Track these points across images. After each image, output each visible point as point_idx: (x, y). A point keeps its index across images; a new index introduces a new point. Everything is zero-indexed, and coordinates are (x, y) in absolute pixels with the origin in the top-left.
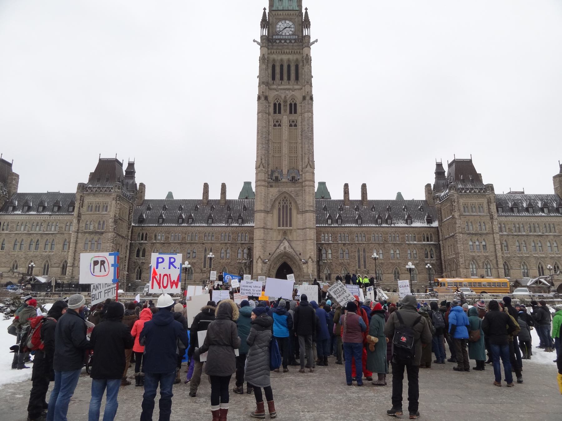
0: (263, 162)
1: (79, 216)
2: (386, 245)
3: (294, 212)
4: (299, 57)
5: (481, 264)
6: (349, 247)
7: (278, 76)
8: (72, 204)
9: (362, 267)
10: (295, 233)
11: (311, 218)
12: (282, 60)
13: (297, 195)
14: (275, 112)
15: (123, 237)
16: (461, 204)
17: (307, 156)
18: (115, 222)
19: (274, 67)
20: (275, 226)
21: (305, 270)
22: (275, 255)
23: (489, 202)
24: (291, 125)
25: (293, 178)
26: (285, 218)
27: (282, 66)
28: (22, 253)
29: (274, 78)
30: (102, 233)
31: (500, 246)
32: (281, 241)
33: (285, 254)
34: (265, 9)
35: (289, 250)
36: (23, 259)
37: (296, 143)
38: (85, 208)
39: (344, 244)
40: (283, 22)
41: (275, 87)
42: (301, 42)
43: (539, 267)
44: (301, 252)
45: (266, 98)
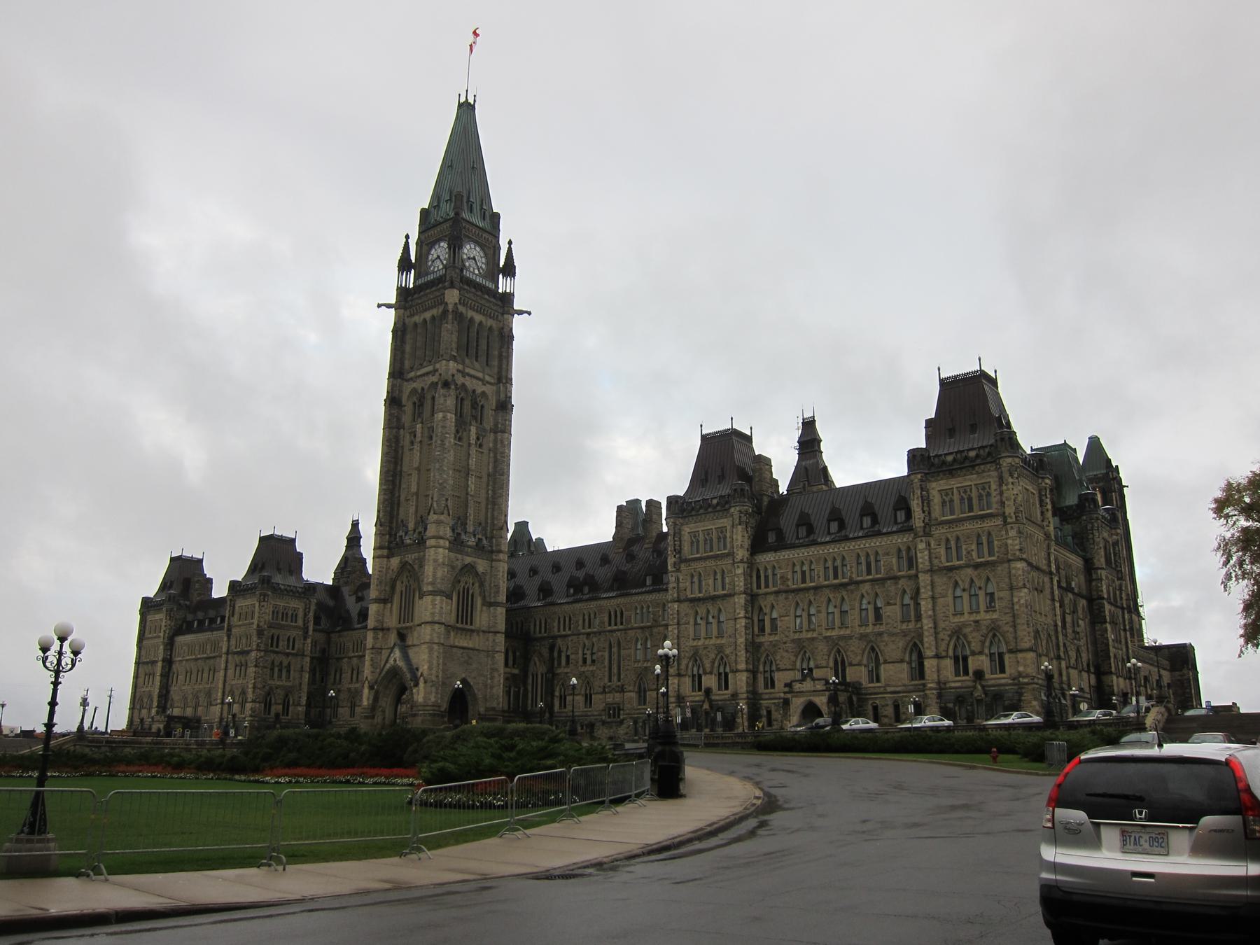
1: (229, 630)
2: (655, 630)
5: (708, 666)
6: (595, 640)
9: (615, 678)
10: (416, 634)
12: (425, 320)
15: (288, 655)
16: (686, 538)
18: (260, 633)
31: (743, 622)
33: (395, 672)
34: (407, 237)
35: (400, 663)
38: (235, 620)
39: (588, 634)
41: (412, 374)
43: (836, 662)
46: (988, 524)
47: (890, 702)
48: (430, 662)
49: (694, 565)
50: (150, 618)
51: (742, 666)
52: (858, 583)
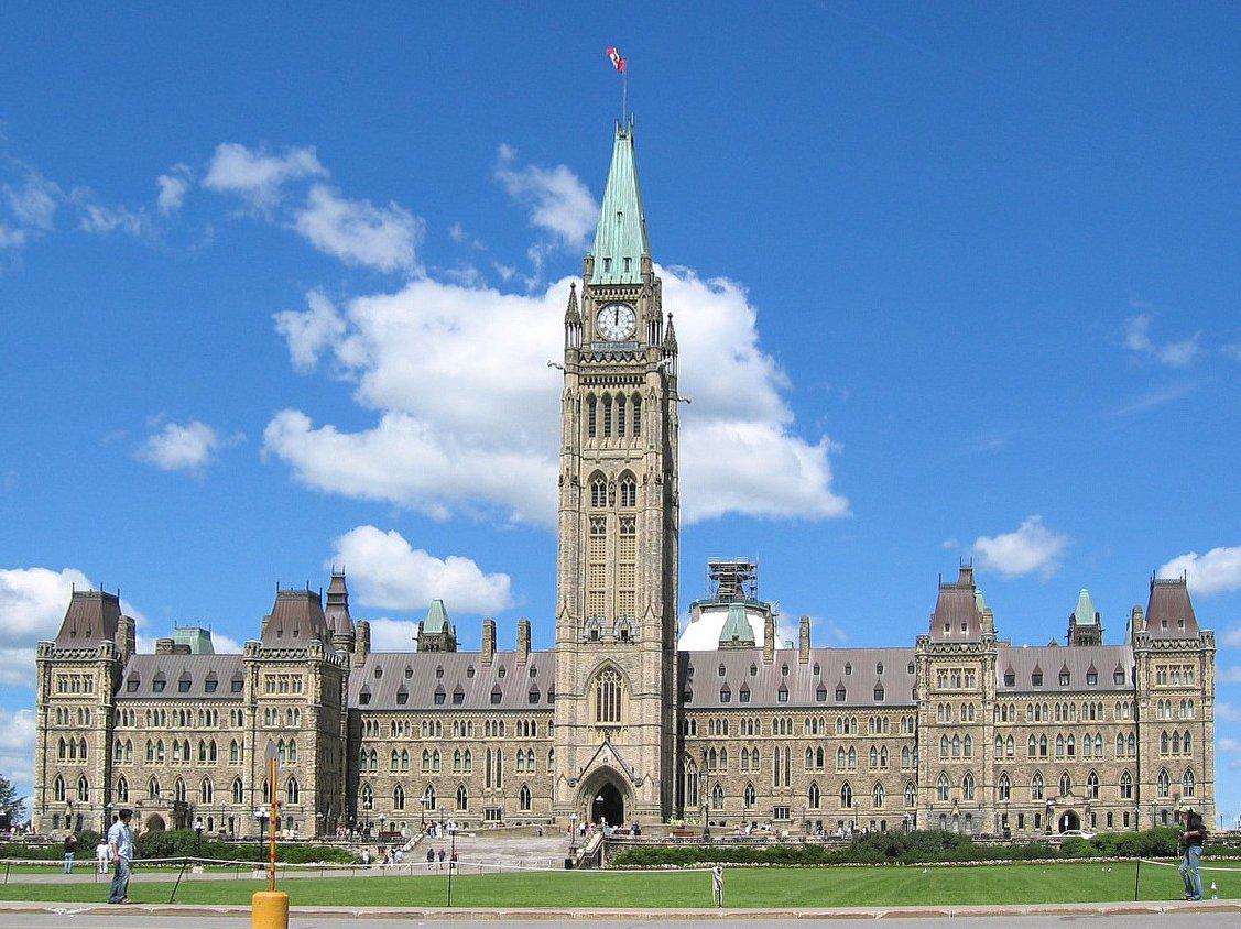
0: (568, 607)
1: (254, 700)
2: (829, 742)
3: (625, 697)
4: (641, 389)
7: (599, 430)
8: (238, 684)
14: (594, 503)
17: (647, 593)
19: (593, 406)
20: (592, 721)
21: (639, 797)
22: (589, 771)
23: (984, 669)
24: (623, 530)
25: (624, 633)
26: (609, 705)
27: (608, 405)
28: (163, 766)
29: (592, 433)
30: (297, 731)
33: (606, 770)
35: (612, 763)
36: (167, 776)
37: (634, 565)
40: (613, 309)
42: (643, 357)
43: (1062, 782)
44: (636, 763)
45: (575, 481)
46: (1190, 694)
47: (1106, 813)
48: (655, 763)
49: (942, 698)
50: (55, 671)
51: (991, 783)
52: (1085, 725)
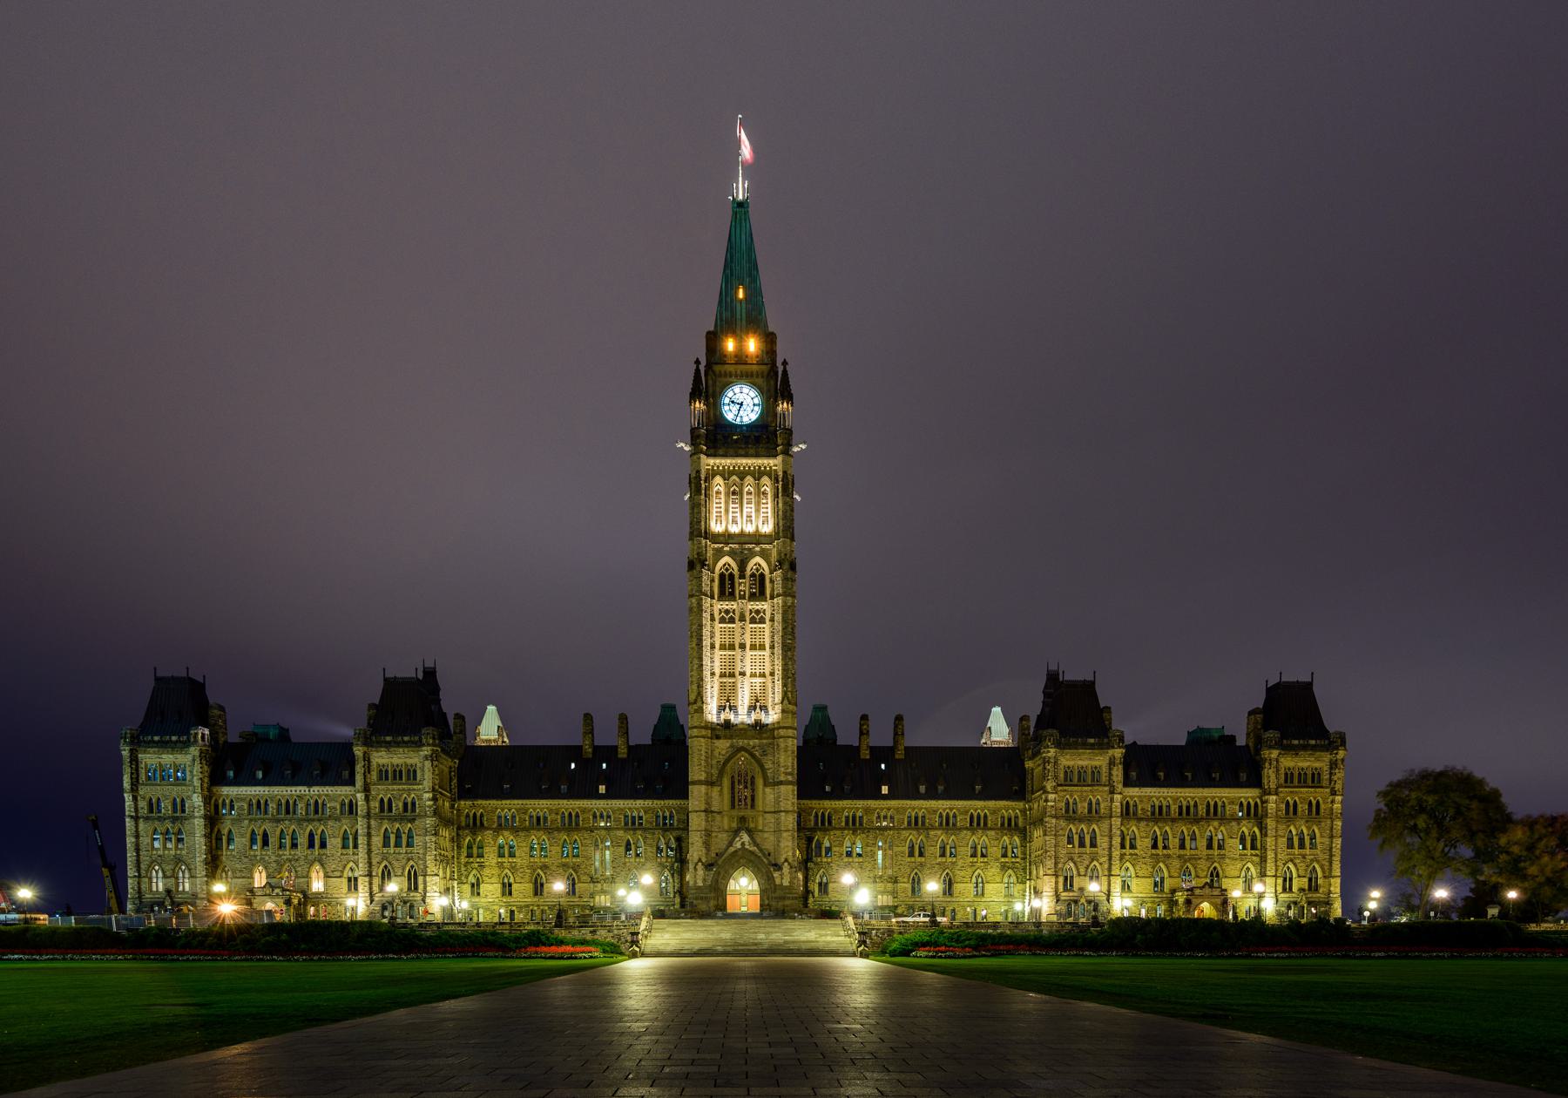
3: (760, 782)
11: (788, 794)
13: (764, 753)
21: (778, 881)
23: (1112, 763)
32: (736, 832)
44: (771, 849)
